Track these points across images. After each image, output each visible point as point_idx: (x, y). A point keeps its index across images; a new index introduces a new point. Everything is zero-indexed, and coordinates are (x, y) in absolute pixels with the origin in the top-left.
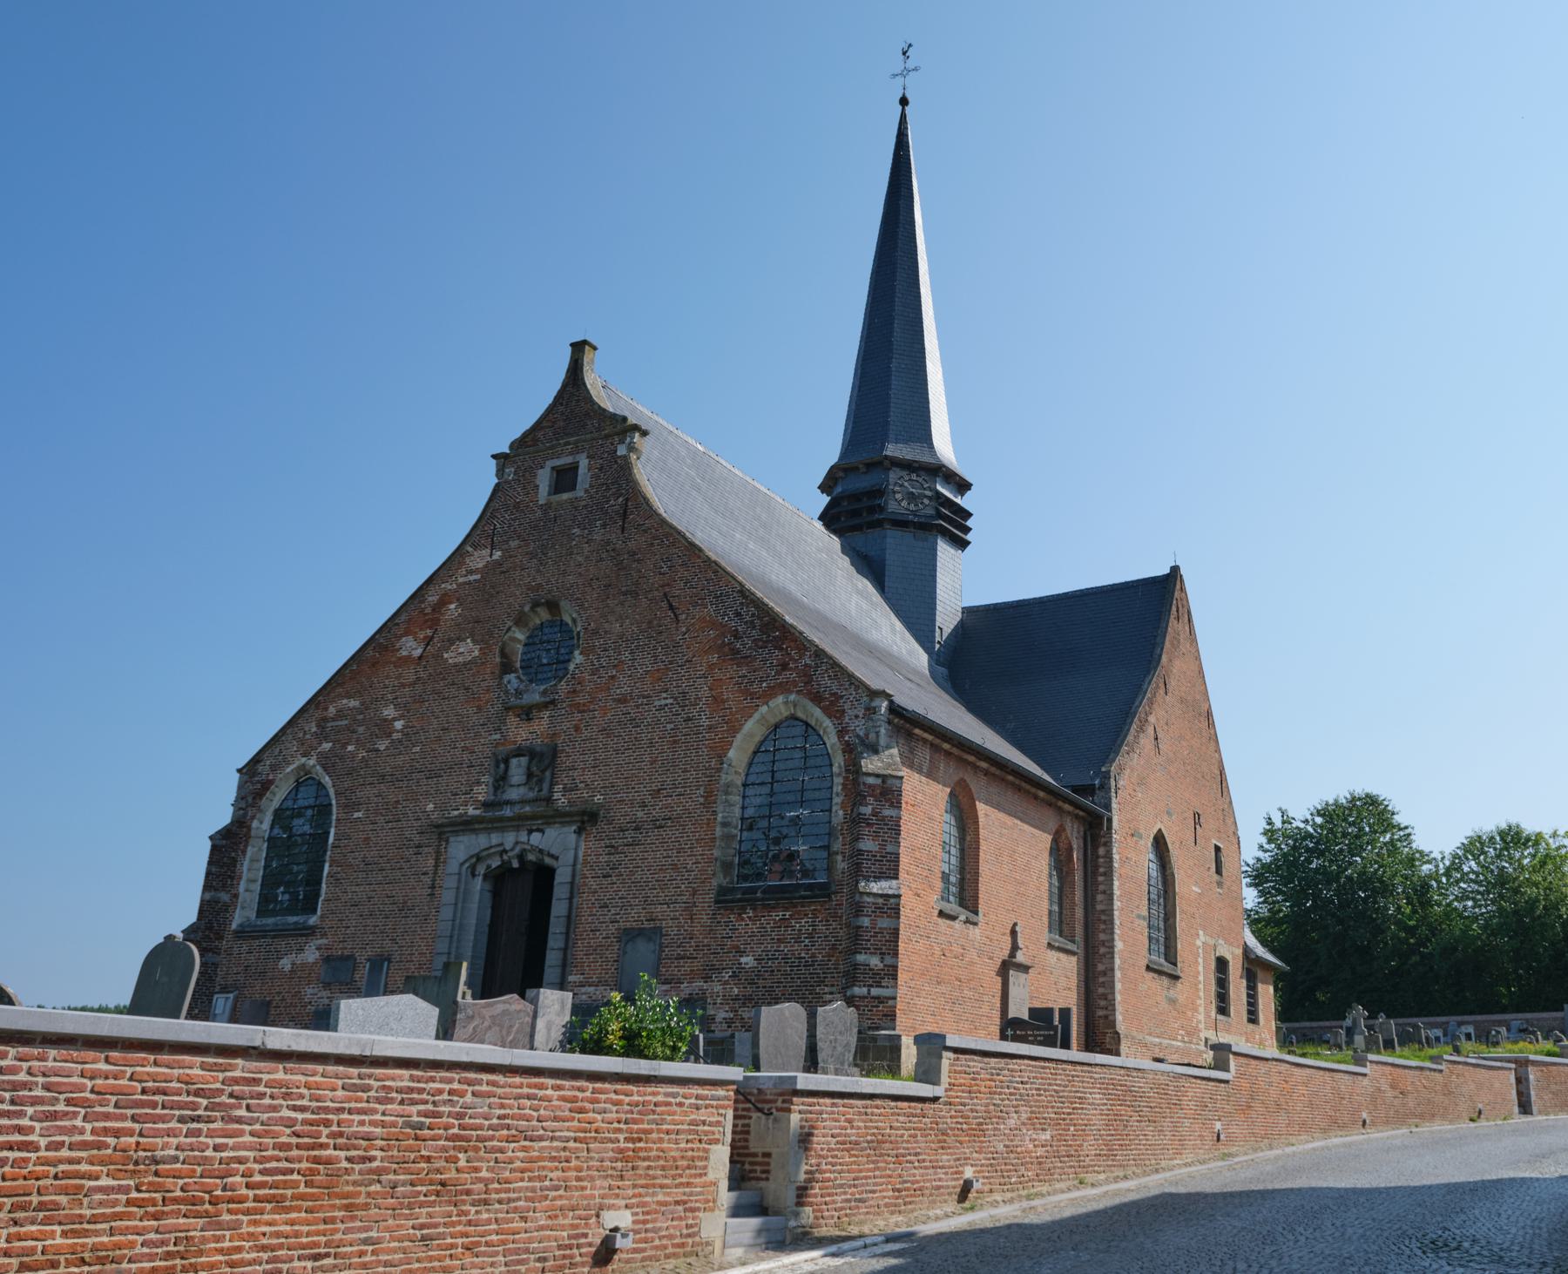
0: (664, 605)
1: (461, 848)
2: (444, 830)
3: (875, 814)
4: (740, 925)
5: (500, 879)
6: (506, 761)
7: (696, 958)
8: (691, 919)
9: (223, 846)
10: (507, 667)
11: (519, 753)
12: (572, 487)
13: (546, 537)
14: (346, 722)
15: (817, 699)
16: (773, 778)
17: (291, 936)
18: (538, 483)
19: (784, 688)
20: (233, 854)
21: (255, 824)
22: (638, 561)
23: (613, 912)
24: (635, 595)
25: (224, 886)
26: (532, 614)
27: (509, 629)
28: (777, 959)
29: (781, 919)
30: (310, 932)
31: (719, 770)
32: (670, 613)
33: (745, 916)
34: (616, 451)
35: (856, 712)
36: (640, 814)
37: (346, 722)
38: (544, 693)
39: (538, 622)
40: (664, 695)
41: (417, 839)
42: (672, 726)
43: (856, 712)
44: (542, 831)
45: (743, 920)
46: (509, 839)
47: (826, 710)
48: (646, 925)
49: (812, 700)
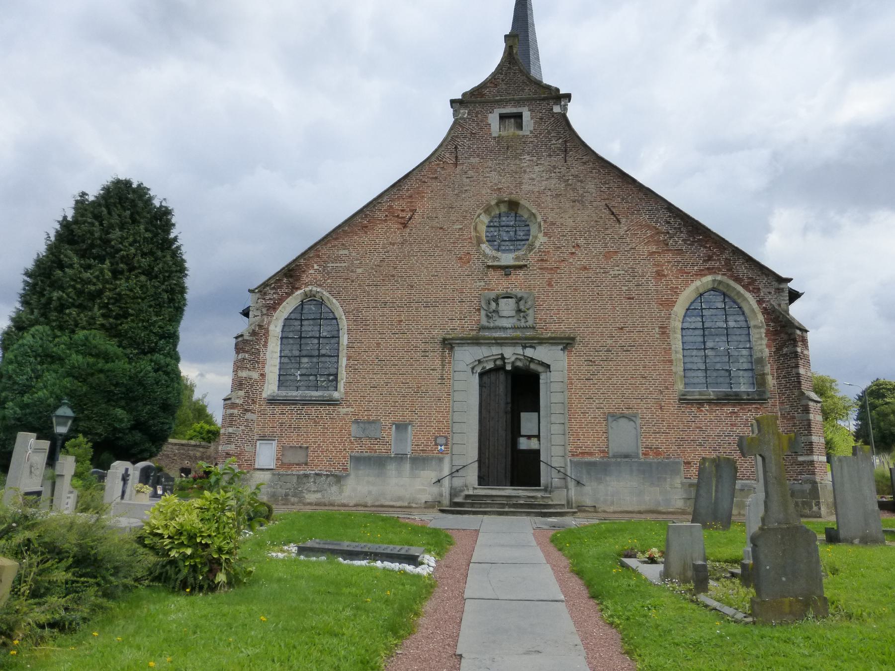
0: (607, 211)
1: (466, 356)
2: (448, 344)
4: (701, 416)
6: (496, 300)
7: (669, 433)
8: (661, 408)
9: (252, 341)
10: (479, 242)
12: (520, 126)
13: (501, 158)
15: (738, 280)
16: (703, 325)
17: (320, 404)
18: (489, 122)
19: (711, 271)
20: (258, 347)
21: (271, 328)
22: (581, 181)
23: (597, 402)
24: (582, 202)
25: (254, 368)
26: (496, 208)
27: (479, 216)
28: (733, 436)
29: (730, 413)
30: (332, 402)
31: (669, 318)
32: (612, 217)
33: (703, 409)
34: (552, 109)
35: (768, 290)
36: (609, 342)
37: (345, 264)
38: (517, 258)
39: (498, 212)
40: (617, 268)
41: (422, 346)
42: (627, 288)
43: (768, 290)
44: (534, 348)
45: (702, 411)
46: (510, 353)
48: (625, 411)
49: (734, 280)
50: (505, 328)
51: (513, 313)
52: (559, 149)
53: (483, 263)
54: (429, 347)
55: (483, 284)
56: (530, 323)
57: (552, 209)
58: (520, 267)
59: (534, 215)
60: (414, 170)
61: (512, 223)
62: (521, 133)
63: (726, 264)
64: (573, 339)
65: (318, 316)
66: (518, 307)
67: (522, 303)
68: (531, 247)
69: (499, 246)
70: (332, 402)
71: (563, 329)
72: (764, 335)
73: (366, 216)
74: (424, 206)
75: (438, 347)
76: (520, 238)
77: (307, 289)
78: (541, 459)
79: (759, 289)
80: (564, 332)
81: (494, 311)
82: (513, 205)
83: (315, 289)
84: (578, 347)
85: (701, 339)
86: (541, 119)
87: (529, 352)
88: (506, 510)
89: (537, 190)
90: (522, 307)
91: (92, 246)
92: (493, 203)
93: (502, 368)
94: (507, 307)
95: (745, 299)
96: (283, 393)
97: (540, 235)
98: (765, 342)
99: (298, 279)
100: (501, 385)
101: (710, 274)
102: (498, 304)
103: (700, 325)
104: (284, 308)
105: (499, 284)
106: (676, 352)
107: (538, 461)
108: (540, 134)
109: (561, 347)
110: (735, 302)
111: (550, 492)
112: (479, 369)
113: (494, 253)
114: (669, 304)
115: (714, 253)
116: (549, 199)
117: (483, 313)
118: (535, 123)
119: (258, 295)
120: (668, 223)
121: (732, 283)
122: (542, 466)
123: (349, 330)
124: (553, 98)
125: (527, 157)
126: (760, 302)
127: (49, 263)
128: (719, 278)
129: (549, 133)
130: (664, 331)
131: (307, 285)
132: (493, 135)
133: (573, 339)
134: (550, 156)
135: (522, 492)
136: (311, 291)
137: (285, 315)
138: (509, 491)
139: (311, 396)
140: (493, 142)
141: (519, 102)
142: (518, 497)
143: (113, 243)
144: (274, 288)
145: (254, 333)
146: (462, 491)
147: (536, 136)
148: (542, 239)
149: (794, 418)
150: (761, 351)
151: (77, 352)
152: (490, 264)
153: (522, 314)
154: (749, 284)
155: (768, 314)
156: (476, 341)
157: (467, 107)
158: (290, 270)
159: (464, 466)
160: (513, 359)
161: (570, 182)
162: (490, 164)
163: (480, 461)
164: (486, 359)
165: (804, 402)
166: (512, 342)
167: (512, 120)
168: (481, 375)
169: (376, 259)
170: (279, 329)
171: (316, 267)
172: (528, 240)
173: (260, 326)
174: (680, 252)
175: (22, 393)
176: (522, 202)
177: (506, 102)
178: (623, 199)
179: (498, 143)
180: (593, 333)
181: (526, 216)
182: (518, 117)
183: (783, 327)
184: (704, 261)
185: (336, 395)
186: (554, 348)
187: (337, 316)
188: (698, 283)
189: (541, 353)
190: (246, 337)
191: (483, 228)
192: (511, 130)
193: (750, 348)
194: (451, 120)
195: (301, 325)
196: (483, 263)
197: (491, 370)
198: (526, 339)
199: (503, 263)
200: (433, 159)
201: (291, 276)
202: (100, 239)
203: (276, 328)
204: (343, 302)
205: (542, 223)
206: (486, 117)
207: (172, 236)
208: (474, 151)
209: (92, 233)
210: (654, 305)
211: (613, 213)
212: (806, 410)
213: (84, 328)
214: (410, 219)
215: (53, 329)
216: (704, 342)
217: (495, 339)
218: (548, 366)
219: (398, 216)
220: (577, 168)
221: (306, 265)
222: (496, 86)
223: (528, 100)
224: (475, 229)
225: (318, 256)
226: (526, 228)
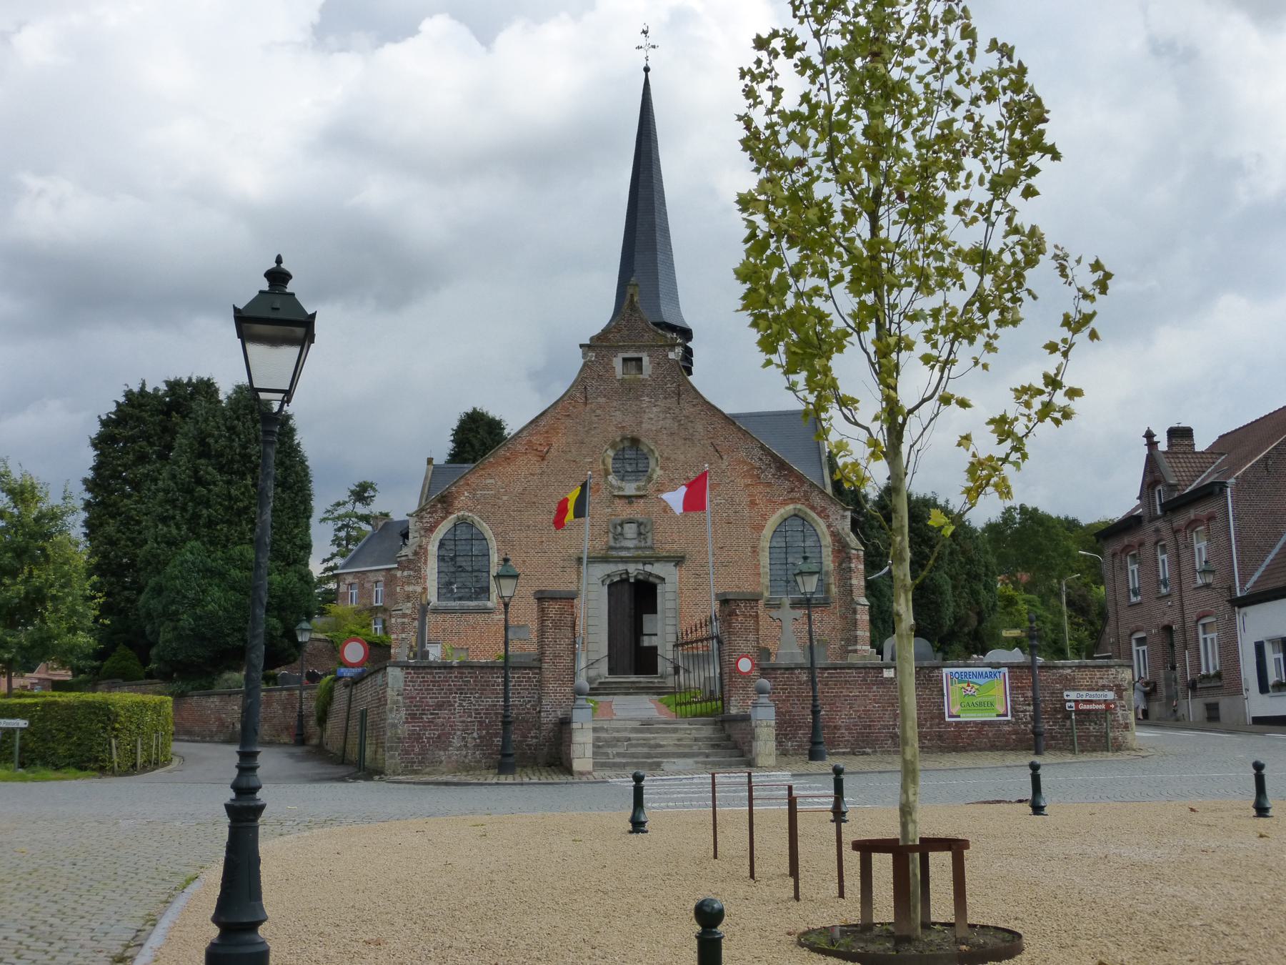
0: (712, 449)
3: (856, 567)
5: (616, 587)
6: (621, 525)
10: (607, 473)
11: (630, 522)
12: (640, 369)
14: (492, 492)
15: (813, 508)
19: (793, 500)
21: (430, 548)
22: (692, 422)
25: (418, 583)
31: (758, 540)
37: (492, 492)
38: (638, 489)
39: (622, 447)
41: (561, 563)
47: (819, 514)
50: (628, 549)
51: (635, 536)
52: (673, 392)
53: (610, 492)
54: (566, 564)
55: (610, 510)
56: (649, 543)
57: (667, 446)
58: (641, 497)
59: (652, 451)
60: (549, 408)
61: (633, 457)
62: (641, 376)
63: (804, 496)
64: (683, 557)
65: (469, 537)
66: (639, 530)
67: (642, 527)
68: (650, 479)
69: (624, 476)
70: (487, 611)
71: (675, 548)
72: (830, 553)
73: (508, 448)
74: (558, 442)
75: (574, 563)
76: (640, 469)
77: (460, 514)
78: (659, 653)
79: (828, 516)
80: (676, 551)
81: (620, 534)
82: (635, 442)
83: (466, 514)
84: (687, 563)
85: (784, 556)
86: (658, 364)
87: (648, 568)
88: (631, 691)
89: (654, 429)
90: (642, 531)
91: (232, 461)
92: (618, 439)
93: (627, 580)
94: (630, 530)
95: (818, 524)
96: (444, 603)
97: (658, 469)
98: (831, 559)
99: (451, 504)
100: (626, 596)
101: (792, 503)
102: (622, 528)
103: (784, 545)
104: (440, 530)
105: (625, 511)
106: (764, 567)
107: (656, 655)
108: (658, 378)
109: (673, 564)
110: (811, 526)
111: (665, 678)
112: (608, 582)
113: (619, 483)
114: (759, 528)
115: (796, 486)
116: (665, 437)
117: (611, 535)
118: (653, 367)
119: (416, 519)
120: (761, 459)
121: (809, 511)
122: (659, 659)
123: (498, 550)
124: (668, 346)
125: (646, 399)
126: (829, 526)
127: (187, 479)
128: (799, 506)
129: (665, 377)
130: (755, 550)
131: (459, 510)
132: (618, 378)
133: (683, 557)
134: (665, 398)
135: (643, 679)
136: (463, 515)
137: (441, 536)
138: (633, 678)
139: (468, 606)
140: (617, 384)
141: (639, 348)
142: (640, 682)
143: (253, 458)
144: (429, 513)
145: (416, 553)
146: (595, 679)
147: (654, 380)
148: (659, 472)
149: (846, 617)
150: (828, 566)
151: (235, 567)
152: (616, 494)
153: (642, 537)
154: (822, 511)
155: (835, 536)
156: (605, 560)
157: (593, 350)
158: (442, 497)
159: (597, 660)
160: (635, 574)
161: (682, 422)
162: (615, 404)
163: (610, 656)
164: (614, 574)
165: (854, 606)
166: (635, 560)
167: (634, 363)
168: (610, 586)
169: (518, 488)
170: (436, 548)
171: (466, 494)
172: (647, 471)
173: (420, 546)
174: (769, 484)
175: (193, 606)
176: (643, 439)
177: (629, 347)
178: (725, 438)
179: (622, 384)
180: (699, 552)
181: (645, 450)
182: (640, 360)
183: (843, 547)
184: (788, 492)
185: (489, 604)
186: (668, 564)
187: (487, 536)
188: (782, 511)
189: (657, 569)
190: (410, 557)
191: (609, 461)
192: (632, 375)
193: (821, 563)
194: (582, 361)
195: (455, 545)
196: (610, 492)
197: (617, 582)
198: (645, 557)
199: (627, 493)
200: (566, 398)
201: (444, 502)
202: (240, 454)
203: (433, 548)
204: (492, 526)
205: (659, 458)
206: (611, 360)
207: (296, 442)
208: (601, 392)
209: (231, 448)
210: (748, 529)
211: (717, 451)
212: (855, 612)
213: (235, 544)
214: (547, 452)
215: (203, 543)
216: (787, 559)
217: (622, 558)
218: (664, 579)
219: (536, 450)
220: (689, 410)
221: (457, 493)
222: (619, 331)
223: (647, 346)
224: (603, 462)
225: (468, 484)
226: (646, 461)
